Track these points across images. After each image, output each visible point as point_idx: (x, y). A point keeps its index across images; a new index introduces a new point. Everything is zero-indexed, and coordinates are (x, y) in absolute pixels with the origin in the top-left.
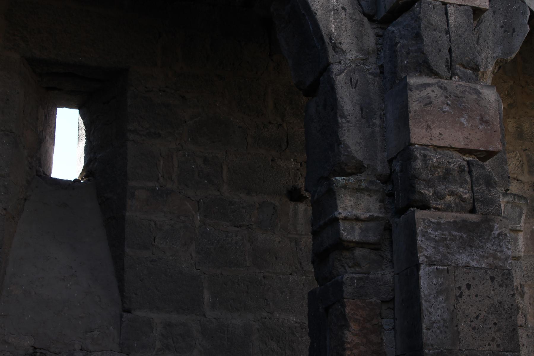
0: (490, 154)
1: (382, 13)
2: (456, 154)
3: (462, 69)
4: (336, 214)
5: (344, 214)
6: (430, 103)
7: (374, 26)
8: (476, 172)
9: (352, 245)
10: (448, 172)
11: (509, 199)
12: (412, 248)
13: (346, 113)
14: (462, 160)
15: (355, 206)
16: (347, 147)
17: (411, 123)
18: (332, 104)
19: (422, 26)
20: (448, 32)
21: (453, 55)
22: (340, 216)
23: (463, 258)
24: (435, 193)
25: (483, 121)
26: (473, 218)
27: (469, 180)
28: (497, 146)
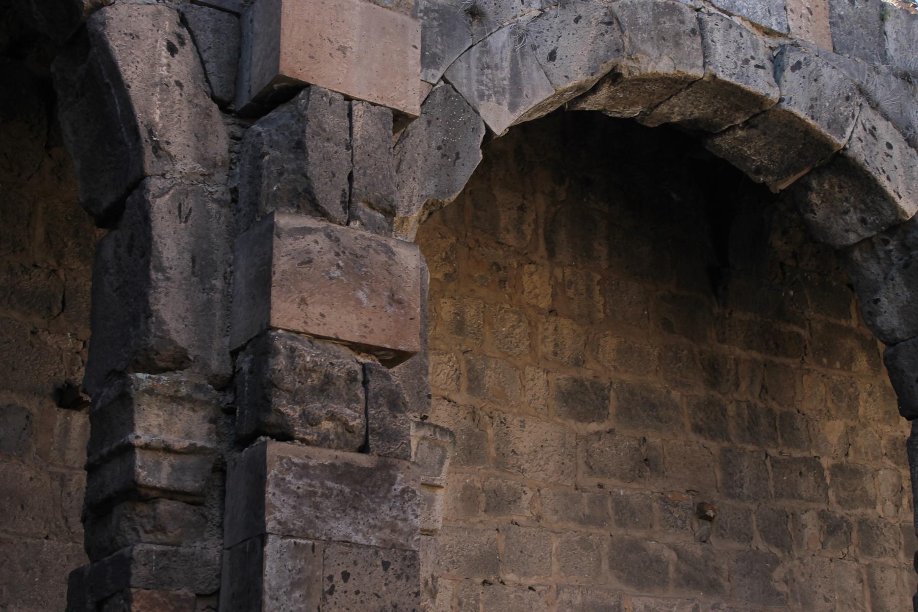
1: (244, 100)
2: (345, 351)
3: (368, 210)
4: (131, 437)
5: (144, 439)
6: (310, 261)
7: (229, 120)
8: (375, 384)
9: (154, 493)
10: (328, 380)
11: (426, 432)
12: (257, 505)
13: (166, 264)
14: (353, 362)
15: (166, 427)
16: (161, 322)
17: (274, 292)
18: (142, 246)
19: (308, 130)
20: (349, 147)
21: (355, 185)
22: (137, 442)
23: (341, 528)
24: (304, 415)
25: (394, 300)
26: (363, 460)
27: (362, 396)
28: (411, 343)
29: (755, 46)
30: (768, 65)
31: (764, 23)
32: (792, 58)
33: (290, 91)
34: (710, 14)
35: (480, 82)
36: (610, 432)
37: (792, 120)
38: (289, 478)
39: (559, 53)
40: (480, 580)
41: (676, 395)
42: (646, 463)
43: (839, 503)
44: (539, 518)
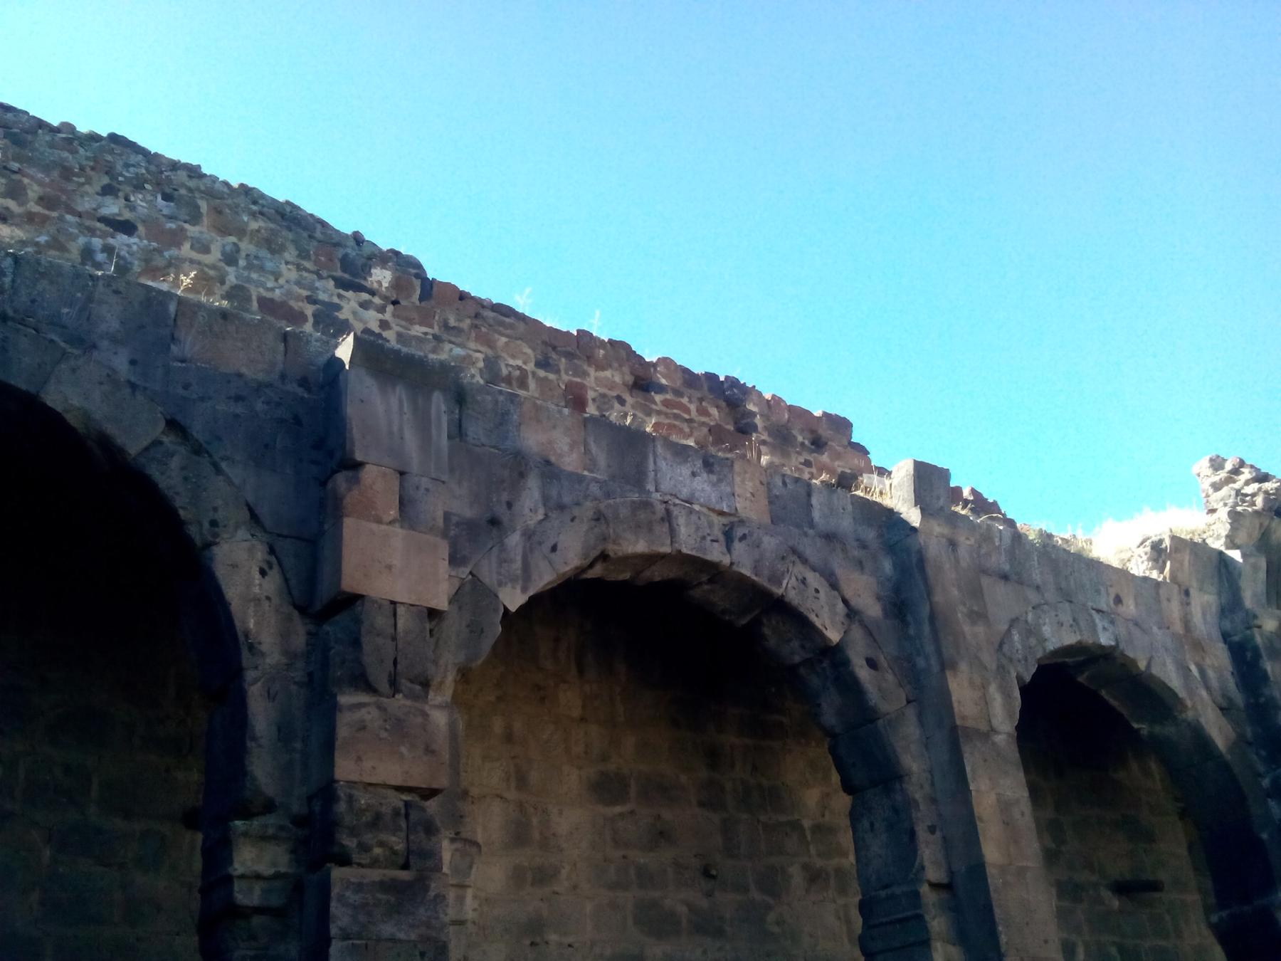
0: (430, 793)
1: (318, 606)
2: (391, 793)
3: (409, 684)
4: (230, 870)
6: (364, 728)
8: (414, 816)
10: (378, 816)
11: (458, 845)
12: (324, 916)
13: (259, 735)
15: (256, 859)
17: (337, 754)
19: (363, 630)
21: (399, 667)
23: (387, 929)
25: (429, 751)
27: (404, 825)
28: (442, 781)
29: (711, 525)
30: (722, 538)
31: (717, 507)
32: (739, 532)
33: (352, 600)
34: (675, 505)
35: (499, 573)
36: (632, 812)
37: (742, 578)
38: (348, 894)
39: (559, 547)
40: (528, 942)
41: (683, 778)
42: (661, 836)
43: (819, 855)
44: (575, 887)
